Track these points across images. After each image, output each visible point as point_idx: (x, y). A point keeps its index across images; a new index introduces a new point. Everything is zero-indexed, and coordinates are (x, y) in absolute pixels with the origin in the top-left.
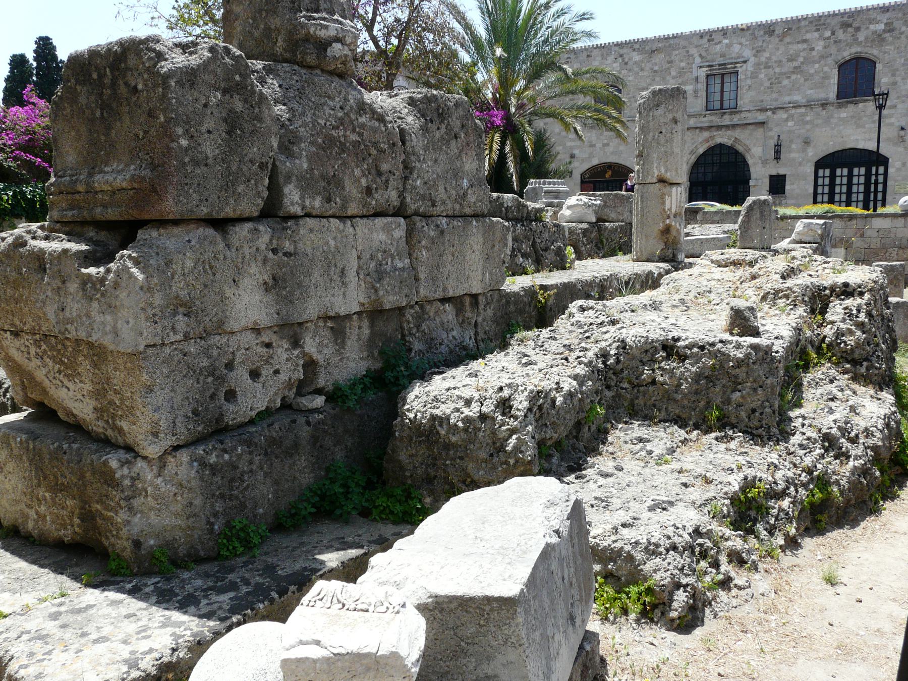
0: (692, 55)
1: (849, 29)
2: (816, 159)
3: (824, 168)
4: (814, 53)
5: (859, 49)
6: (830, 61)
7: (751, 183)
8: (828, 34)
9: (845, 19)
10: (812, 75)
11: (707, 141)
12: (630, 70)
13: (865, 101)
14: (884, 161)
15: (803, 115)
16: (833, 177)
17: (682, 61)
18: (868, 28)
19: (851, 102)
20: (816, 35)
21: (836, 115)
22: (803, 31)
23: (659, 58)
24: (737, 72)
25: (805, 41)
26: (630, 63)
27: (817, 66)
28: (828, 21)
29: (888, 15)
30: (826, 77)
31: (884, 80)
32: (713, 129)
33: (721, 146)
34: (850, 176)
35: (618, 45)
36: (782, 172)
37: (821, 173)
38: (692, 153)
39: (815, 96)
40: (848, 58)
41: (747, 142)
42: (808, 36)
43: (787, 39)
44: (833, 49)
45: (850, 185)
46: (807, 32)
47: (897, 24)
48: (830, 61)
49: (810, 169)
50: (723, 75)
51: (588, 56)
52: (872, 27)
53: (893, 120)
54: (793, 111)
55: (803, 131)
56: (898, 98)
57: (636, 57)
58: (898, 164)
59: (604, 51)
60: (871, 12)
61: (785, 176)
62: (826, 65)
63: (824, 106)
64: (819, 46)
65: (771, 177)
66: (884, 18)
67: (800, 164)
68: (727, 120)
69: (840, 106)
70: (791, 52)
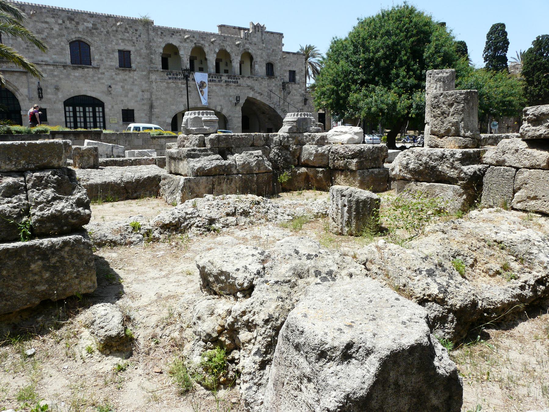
1: (73, 22)
2: (64, 100)
3: (69, 106)
4: (53, 32)
5: (80, 36)
6: (64, 39)
7: (22, 113)
8: (60, 21)
9: (69, 15)
10: (54, 46)
13: (88, 68)
14: (101, 104)
15: (52, 71)
16: (74, 111)
18: (83, 24)
19: (80, 67)
20: (53, 20)
21: (72, 74)
22: (44, 16)
25: (46, 22)
27: (56, 40)
28: (59, 13)
29: (93, 19)
30: (63, 49)
31: (97, 57)
37: (67, 108)
39: (58, 60)
40: (74, 40)
41: (16, 84)
42: (48, 20)
43: (34, 18)
44: (65, 32)
45: (85, 117)
46: (47, 17)
47: (99, 26)
48: (64, 39)
49: (61, 106)
52: (85, 24)
53: (104, 81)
54: (45, 67)
55: (53, 81)
56: (105, 69)
58: (110, 107)
60: (84, 15)
62: (62, 41)
63: (65, 66)
64: (56, 28)
66: (92, 20)
67: (55, 103)
69: (74, 68)
70: (38, 27)
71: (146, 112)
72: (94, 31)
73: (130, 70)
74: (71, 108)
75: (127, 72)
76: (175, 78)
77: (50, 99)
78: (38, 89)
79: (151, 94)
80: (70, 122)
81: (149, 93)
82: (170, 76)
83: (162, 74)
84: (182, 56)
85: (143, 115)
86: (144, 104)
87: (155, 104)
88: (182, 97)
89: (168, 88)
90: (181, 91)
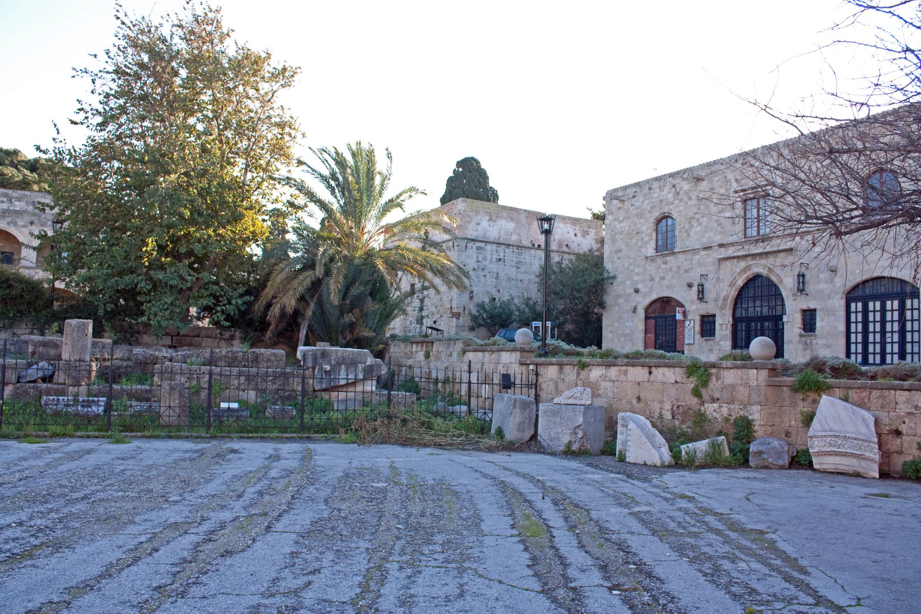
0: (729, 181)
3: (856, 300)
11: (744, 271)
12: (681, 200)
16: (865, 312)
17: (721, 187)
23: (704, 185)
26: (681, 193)
32: (749, 258)
33: (757, 277)
34: (883, 311)
35: (671, 175)
36: (812, 306)
37: (853, 305)
38: (732, 285)
45: (883, 322)
49: (839, 303)
51: (650, 189)
57: (686, 186)
59: (661, 183)
61: (815, 310)
67: (829, 297)
77: (822, 291)
78: (799, 276)
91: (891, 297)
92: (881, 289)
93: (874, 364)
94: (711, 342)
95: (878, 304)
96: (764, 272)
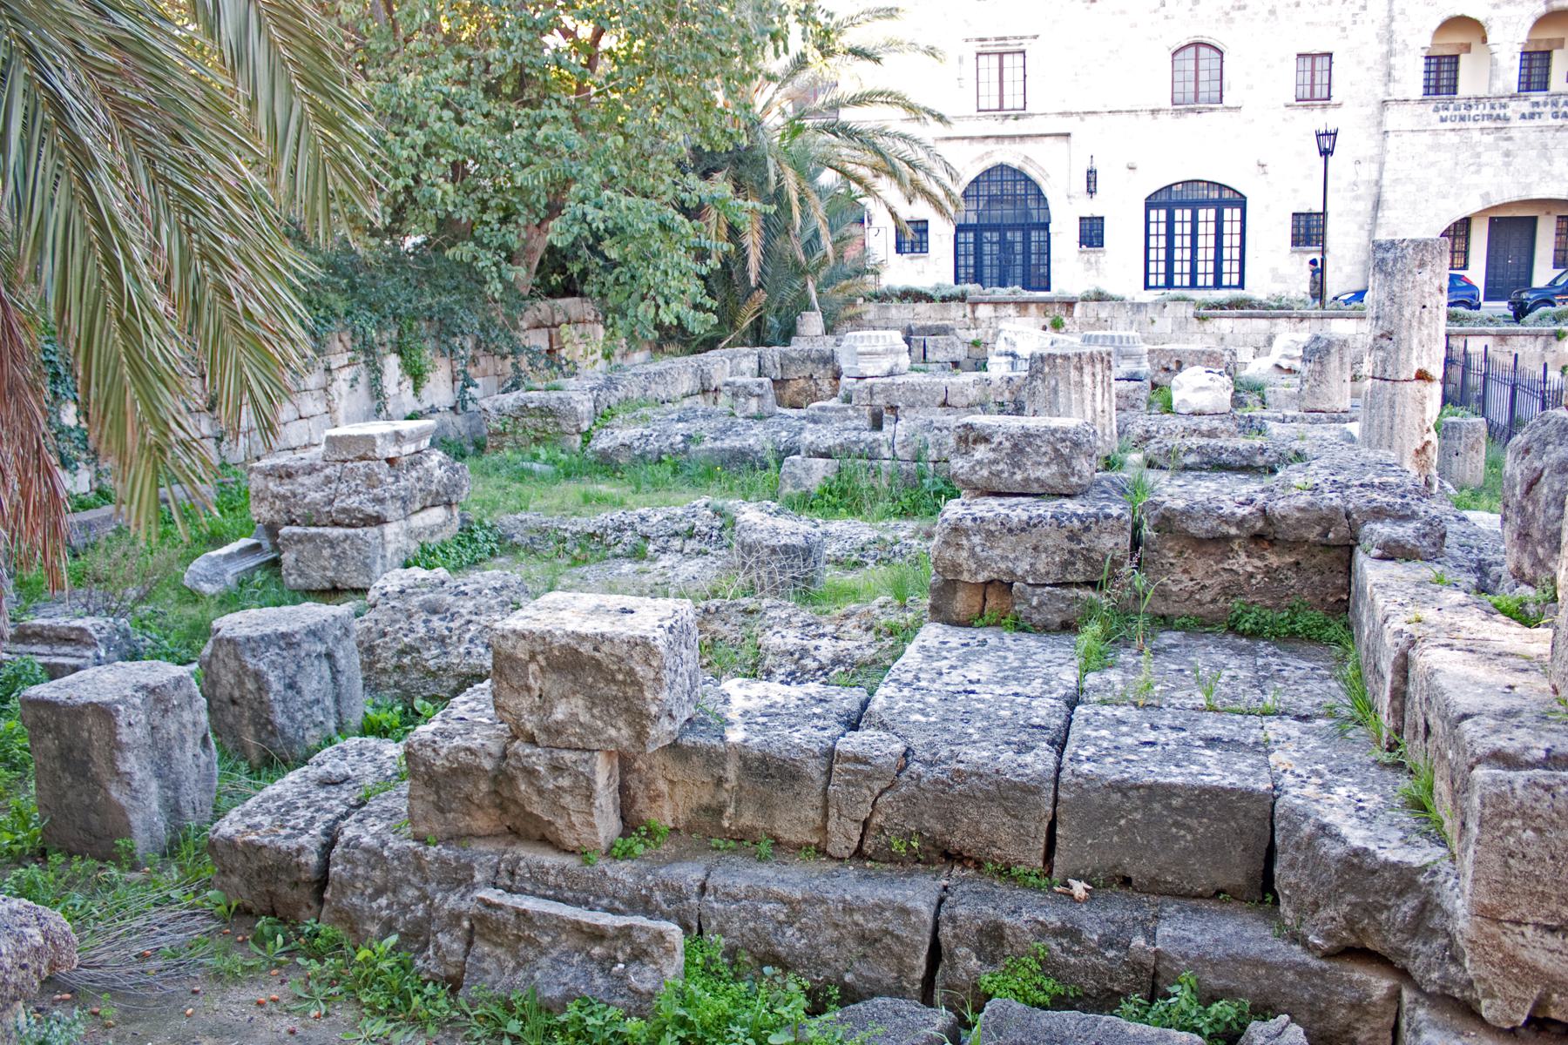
3: (1158, 206)
11: (981, 158)
14: (1240, 202)
19: (1193, 110)
24: (1023, 52)
33: (1002, 167)
34: (1194, 222)
37: (1153, 213)
50: (1001, 54)
65: (1081, 219)
68: (1011, 127)
71: (1360, 219)
72: (1235, 14)
73: (1324, 106)
74: (1163, 214)
75: (1317, 112)
76: (1462, 119)
79: (1382, 165)
80: (966, 266)
81: (1375, 167)
82: (1444, 114)
83: (1421, 109)
84: (1494, 48)
85: (1355, 227)
86: (1357, 198)
87: (1388, 195)
88: (1478, 172)
89: (1436, 147)
90: (1478, 155)
91: (1206, 204)
92: (1202, 194)
93: (1205, 287)
94: (921, 261)
95: (1188, 214)
96: (1015, 164)
